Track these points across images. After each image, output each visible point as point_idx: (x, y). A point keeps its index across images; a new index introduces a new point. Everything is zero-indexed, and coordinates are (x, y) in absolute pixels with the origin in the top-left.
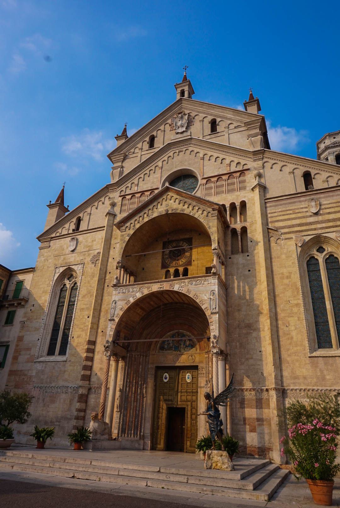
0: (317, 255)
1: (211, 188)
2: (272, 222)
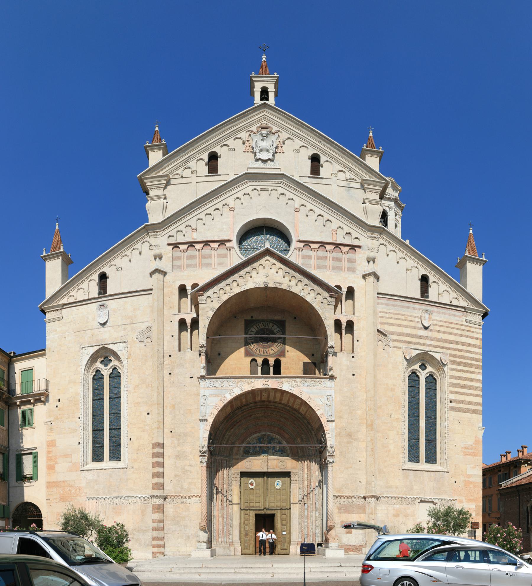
2: (382, 323)
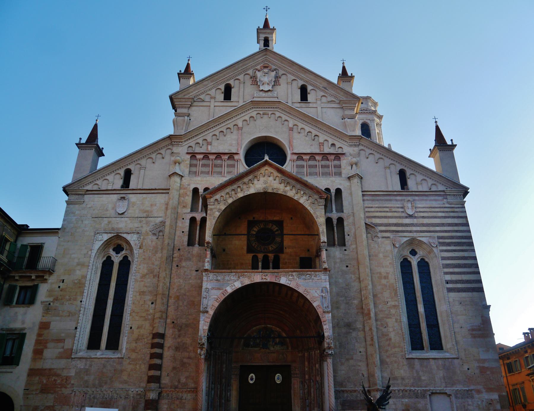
0: (410, 258)
1: (303, 167)
